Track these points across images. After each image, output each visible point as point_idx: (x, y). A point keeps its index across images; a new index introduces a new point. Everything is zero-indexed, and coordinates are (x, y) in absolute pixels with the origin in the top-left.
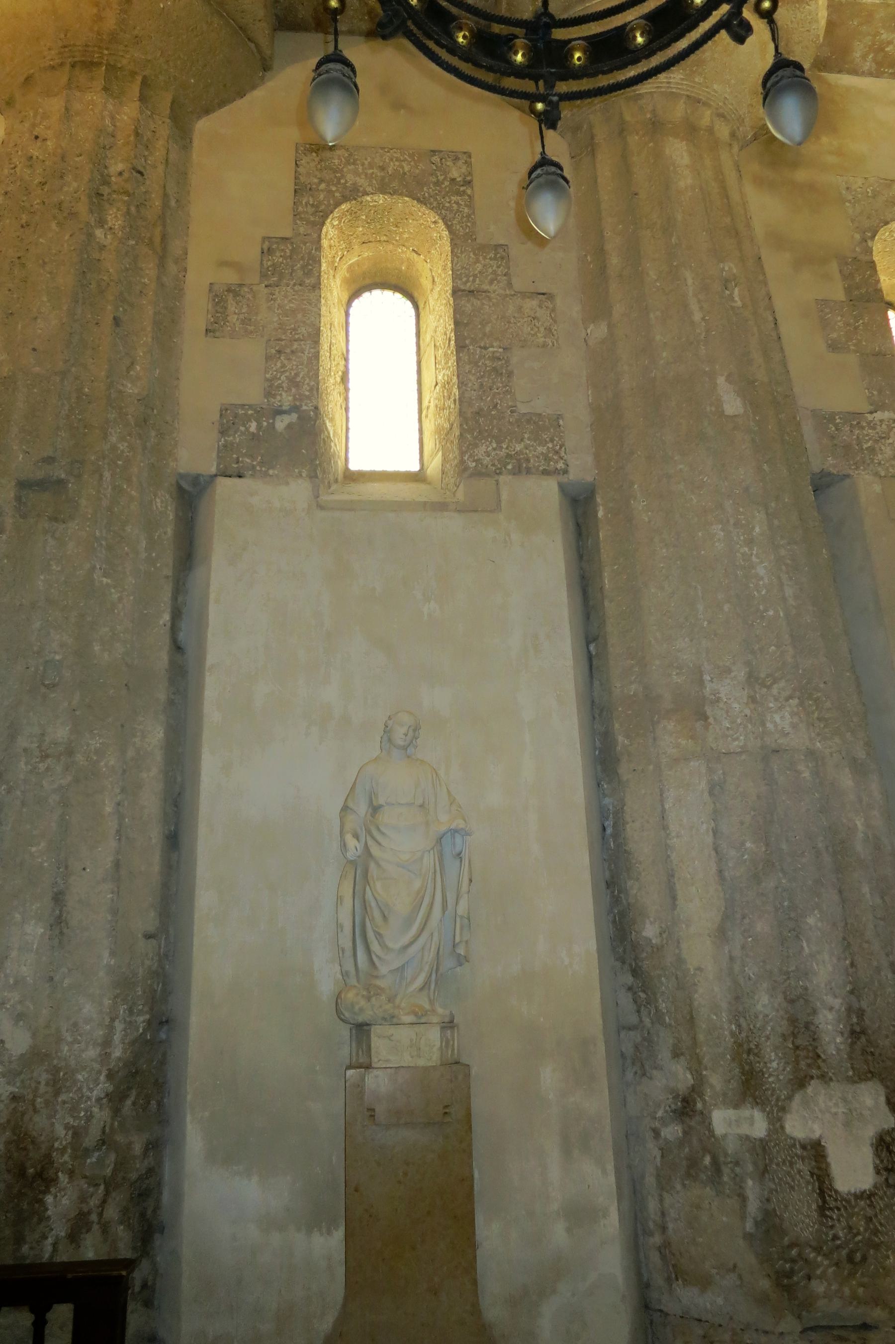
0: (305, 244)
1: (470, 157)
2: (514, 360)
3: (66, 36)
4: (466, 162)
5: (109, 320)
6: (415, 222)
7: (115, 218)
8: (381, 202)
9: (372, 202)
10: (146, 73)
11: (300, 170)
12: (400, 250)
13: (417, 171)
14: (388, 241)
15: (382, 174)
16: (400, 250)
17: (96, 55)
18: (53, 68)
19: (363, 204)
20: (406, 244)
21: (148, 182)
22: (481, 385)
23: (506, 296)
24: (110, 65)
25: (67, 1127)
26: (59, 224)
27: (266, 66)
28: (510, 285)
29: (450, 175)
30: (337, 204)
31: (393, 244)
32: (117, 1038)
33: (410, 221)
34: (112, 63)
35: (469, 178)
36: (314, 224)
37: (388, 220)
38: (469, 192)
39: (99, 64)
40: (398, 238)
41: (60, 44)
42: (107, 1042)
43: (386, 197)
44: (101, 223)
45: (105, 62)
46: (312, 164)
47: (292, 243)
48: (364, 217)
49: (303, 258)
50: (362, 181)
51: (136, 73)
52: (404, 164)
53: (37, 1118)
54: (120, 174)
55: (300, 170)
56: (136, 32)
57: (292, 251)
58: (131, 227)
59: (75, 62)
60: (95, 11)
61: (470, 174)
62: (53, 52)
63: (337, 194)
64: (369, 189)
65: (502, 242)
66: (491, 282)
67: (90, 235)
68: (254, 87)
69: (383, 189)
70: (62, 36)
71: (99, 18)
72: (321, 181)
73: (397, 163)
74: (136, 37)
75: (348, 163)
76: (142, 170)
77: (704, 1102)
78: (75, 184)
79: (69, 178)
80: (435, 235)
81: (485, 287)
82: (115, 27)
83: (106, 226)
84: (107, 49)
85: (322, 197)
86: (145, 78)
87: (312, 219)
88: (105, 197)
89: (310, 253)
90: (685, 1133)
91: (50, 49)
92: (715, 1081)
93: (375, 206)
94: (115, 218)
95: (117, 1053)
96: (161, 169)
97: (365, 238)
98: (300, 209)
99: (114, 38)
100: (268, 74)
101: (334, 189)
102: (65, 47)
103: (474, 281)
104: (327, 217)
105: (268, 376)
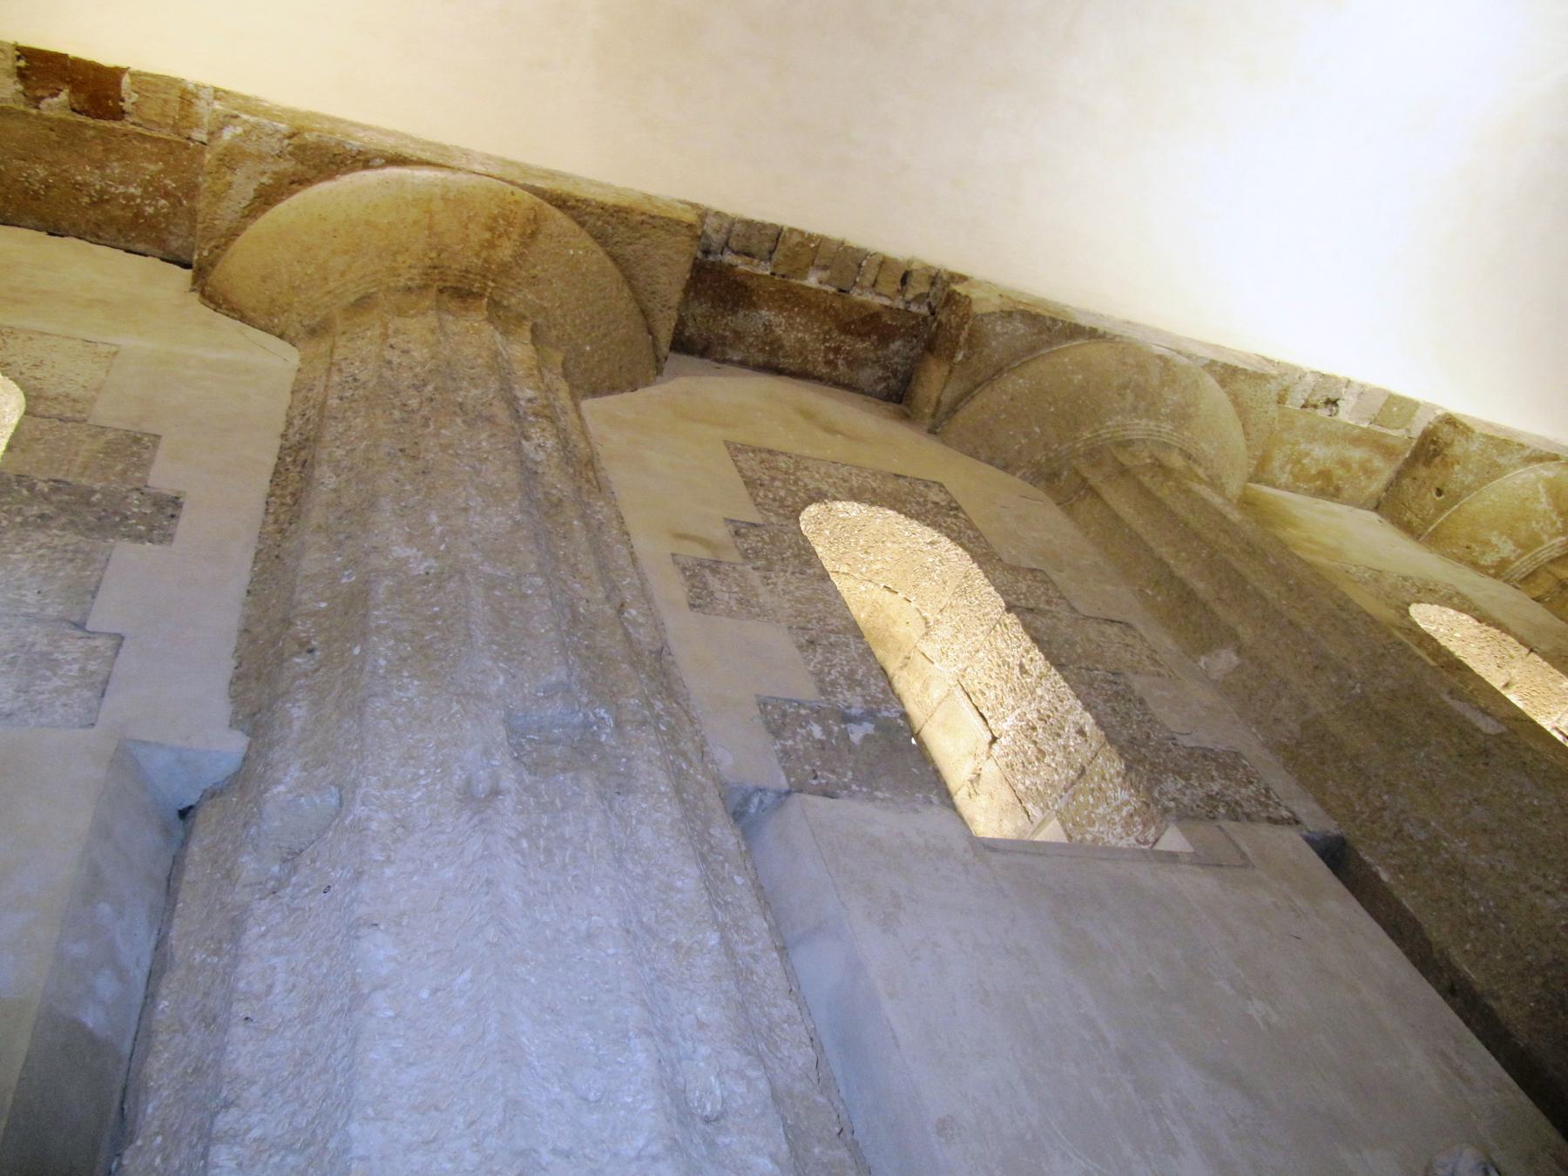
3: (439, 255)
6: (896, 546)
8: (854, 514)
9: (842, 512)
10: (539, 320)
12: (863, 589)
14: (848, 574)
16: (863, 589)
17: (477, 285)
18: (409, 289)
19: (832, 513)
20: (876, 579)
24: (494, 301)
27: (658, 367)
31: (855, 579)
33: (889, 545)
34: (497, 298)
37: (857, 543)
39: (481, 296)
40: (864, 570)
41: (428, 262)
43: (862, 508)
45: (488, 295)
48: (827, 532)
51: (524, 317)
56: (533, 272)
59: (445, 288)
60: (488, 235)
62: (414, 271)
68: (647, 385)
69: (855, 496)
70: (433, 255)
71: (491, 245)
74: (534, 277)
80: (931, 560)
82: (510, 259)
84: (493, 281)
86: (535, 325)
91: (410, 267)
93: (844, 520)
99: (505, 269)
100: (658, 378)
102: (435, 268)
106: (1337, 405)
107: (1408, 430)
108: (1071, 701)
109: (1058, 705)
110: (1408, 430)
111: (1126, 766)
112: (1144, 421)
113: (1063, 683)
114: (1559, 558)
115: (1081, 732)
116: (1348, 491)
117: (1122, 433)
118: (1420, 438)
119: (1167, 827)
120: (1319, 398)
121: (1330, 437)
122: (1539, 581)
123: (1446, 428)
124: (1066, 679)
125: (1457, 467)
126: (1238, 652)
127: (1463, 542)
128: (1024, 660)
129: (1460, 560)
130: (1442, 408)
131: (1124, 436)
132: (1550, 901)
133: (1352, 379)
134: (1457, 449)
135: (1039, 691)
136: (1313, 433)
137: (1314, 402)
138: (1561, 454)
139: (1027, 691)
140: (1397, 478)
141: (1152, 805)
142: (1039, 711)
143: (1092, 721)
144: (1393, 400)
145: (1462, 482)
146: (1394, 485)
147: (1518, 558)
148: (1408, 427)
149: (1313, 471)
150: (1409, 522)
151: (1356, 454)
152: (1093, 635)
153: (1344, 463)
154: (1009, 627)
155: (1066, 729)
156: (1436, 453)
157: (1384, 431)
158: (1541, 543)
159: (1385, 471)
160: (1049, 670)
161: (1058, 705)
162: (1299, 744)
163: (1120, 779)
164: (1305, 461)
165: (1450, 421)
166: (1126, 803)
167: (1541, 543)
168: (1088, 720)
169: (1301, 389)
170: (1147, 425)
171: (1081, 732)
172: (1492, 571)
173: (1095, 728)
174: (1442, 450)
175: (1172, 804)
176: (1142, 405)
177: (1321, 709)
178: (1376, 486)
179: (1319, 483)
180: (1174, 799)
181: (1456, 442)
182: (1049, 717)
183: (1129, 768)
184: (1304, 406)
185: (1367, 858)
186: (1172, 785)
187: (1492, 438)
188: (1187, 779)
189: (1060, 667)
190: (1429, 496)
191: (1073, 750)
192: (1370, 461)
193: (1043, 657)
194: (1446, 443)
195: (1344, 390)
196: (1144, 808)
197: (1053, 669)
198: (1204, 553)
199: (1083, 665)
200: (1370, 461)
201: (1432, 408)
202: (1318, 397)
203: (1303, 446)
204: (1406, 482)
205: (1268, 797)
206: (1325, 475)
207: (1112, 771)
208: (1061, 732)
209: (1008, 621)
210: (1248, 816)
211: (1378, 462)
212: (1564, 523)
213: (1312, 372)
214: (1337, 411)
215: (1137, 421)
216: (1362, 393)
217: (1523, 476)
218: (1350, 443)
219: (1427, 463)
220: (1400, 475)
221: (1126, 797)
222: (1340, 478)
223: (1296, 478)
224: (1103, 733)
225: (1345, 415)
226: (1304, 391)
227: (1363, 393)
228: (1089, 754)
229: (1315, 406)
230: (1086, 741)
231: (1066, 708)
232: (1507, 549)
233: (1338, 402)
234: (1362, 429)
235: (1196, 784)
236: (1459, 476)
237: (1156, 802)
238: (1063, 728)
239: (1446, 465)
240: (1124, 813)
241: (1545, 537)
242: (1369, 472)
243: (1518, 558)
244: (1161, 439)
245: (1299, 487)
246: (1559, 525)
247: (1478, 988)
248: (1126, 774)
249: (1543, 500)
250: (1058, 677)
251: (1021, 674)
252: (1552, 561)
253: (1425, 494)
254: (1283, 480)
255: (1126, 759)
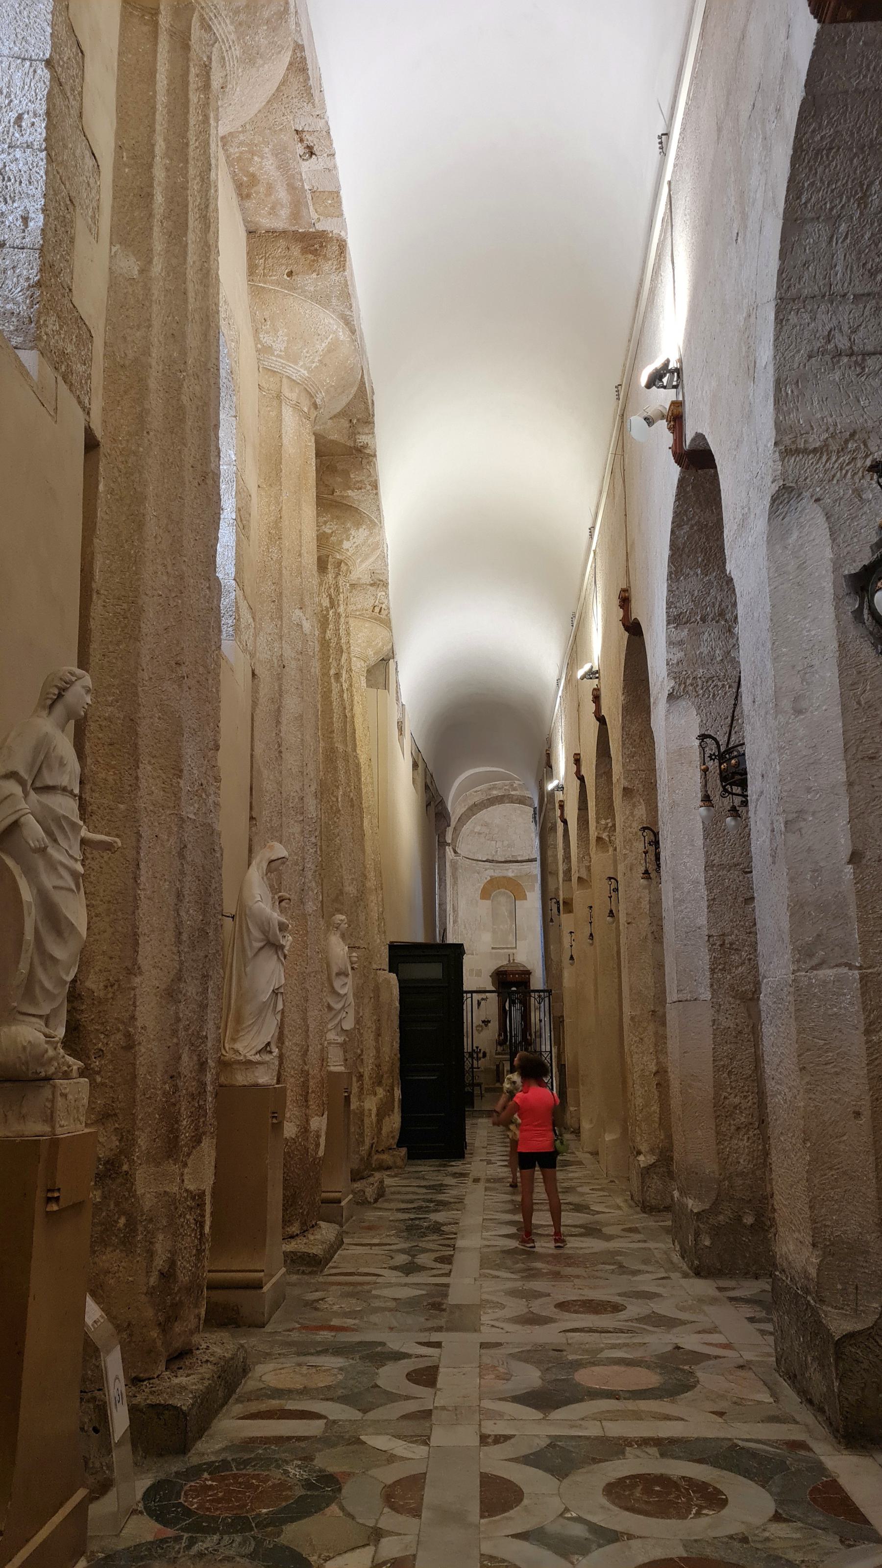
77: (132, 1162)
90: (104, 1197)
92: (143, 1141)
106: (311, 156)
107: (319, 219)
108: (38, 190)
109: (25, 182)
110: (319, 219)
111: (39, 281)
112: (231, 28)
113: (42, 173)
114: (294, 380)
115: (25, 220)
116: (250, 204)
117: (212, 15)
118: (318, 232)
119: (32, 348)
120: (310, 139)
121: (283, 166)
122: (272, 379)
123: (335, 247)
124: (46, 173)
125: (314, 275)
126: (142, 271)
127: (267, 314)
128: (26, 116)
129: (253, 321)
130: (347, 234)
131: (211, 19)
132: (165, 578)
133: (336, 156)
134: (326, 267)
135: (18, 153)
136: (280, 152)
137: (305, 138)
138: (357, 332)
139: (8, 141)
140: (281, 233)
141: (33, 325)
142: (5, 166)
143: (41, 224)
144: (335, 195)
145: (305, 285)
146: (275, 234)
147: (278, 356)
148: (322, 218)
149: (251, 170)
150: (257, 266)
151: (282, 194)
152: (78, 152)
153: (270, 188)
154: (37, 77)
155: (16, 205)
156: (315, 252)
157: (310, 203)
158: (296, 363)
159: (280, 223)
160: (41, 151)
161: (25, 182)
162: (123, 366)
163: (26, 284)
164: (256, 158)
165: (342, 247)
166: (18, 304)
167: (296, 363)
168: (37, 221)
169: (309, 121)
170: (230, 33)
171: (25, 220)
172: (259, 346)
173: (39, 232)
174: (319, 255)
175: (45, 337)
176: (242, 17)
177: (154, 364)
178: (266, 222)
179: (245, 179)
180: (47, 334)
181: (330, 262)
182: (9, 180)
183: (39, 284)
184: (297, 131)
185: (101, 469)
186: (52, 324)
187: (346, 285)
188: (61, 327)
189: (50, 159)
190: (284, 267)
191: (7, 223)
192: (282, 206)
193: (44, 135)
194: (325, 255)
195: (325, 155)
196: (27, 321)
197: (44, 153)
198: (180, 180)
199: (60, 171)
200: (282, 206)
201: (344, 227)
202: (310, 139)
203: (267, 150)
204: (282, 243)
205: (86, 383)
206: (254, 180)
207: (25, 272)
208: (9, 201)
209: (39, 71)
210: (72, 384)
211: (284, 213)
212: (316, 367)
213: (327, 122)
214: (307, 160)
215: (228, 21)
216: (330, 171)
217: (332, 321)
218: (287, 185)
219: (305, 251)
220: (284, 233)
221: (20, 299)
222: (258, 193)
223: (239, 159)
224: (41, 242)
225: (307, 167)
226: (310, 125)
227: (331, 171)
228: (18, 242)
229: (301, 141)
230: (24, 231)
231: (29, 192)
232: (279, 346)
233: (314, 156)
234: (303, 186)
235: (62, 336)
236: (309, 281)
237: (38, 328)
238: (14, 202)
239: (312, 267)
240: (8, 307)
241: (301, 363)
242: (273, 211)
243: (278, 356)
244: (225, 54)
245: (233, 166)
246: (314, 365)
247: (94, 586)
248: (33, 286)
249: (324, 345)
250: (43, 164)
251: (14, 123)
252: (288, 377)
253: (282, 264)
254: (231, 150)
255: (42, 276)
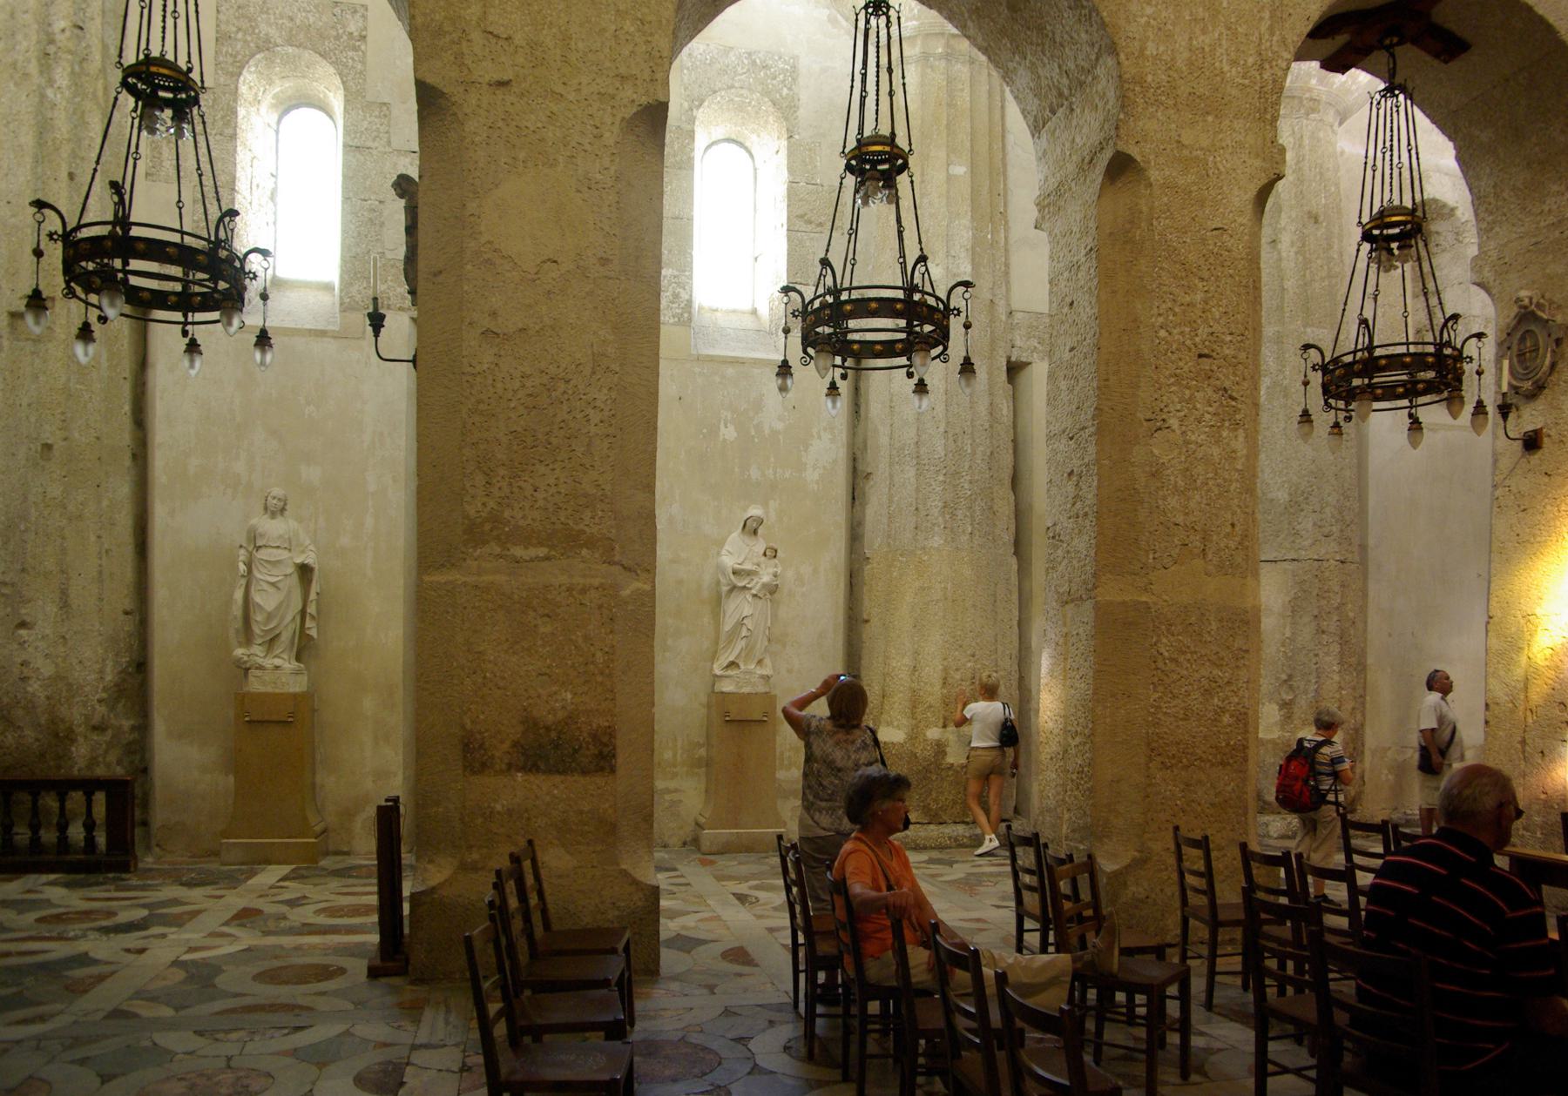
0: (224, 94)
1: (367, 10)
2: (386, 213)
4: (363, 16)
5: (64, 175)
7: (62, 77)
11: (222, 17)
13: (321, 24)
15: (290, 25)
21: (88, 36)
22: (359, 233)
23: (385, 153)
25: (81, 715)
26: (16, 84)
28: (389, 143)
29: (348, 30)
30: (252, 56)
32: (108, 670)
35: (364, 33)
36: (232, 74)
38: (363, 47)
42: (101, 671)
44: (51, 82)
46: (231, 11)
47: (214, 93)
49: (222, 109)
50: (273, 32)
52: (309, 15)
53: (62, 709)
54: (63, 31)
55: (222, 17)
57: (214, 100)
58: (76, 84)
61: (365, 28)
63: (252, 45)
64: (279, 41)
65: (386, 101)
66: (374, 140)
67: (43, 96)
72: (239, 29)
73: (304, 14)
75: (262, 12)
76: (81, 24)
78: (25, 44)
79: (19, 37)
81: (369, 144)
83: (56, 86)
85: (239, 47)
87: (231, 70)
88: (52, 57)
89: (228, 104)
94: (62, 77)
95: (109, 678)
96: (98, 21)
97: (283, 75)
98: (221, 59)
101: (249, 39)
103: (361, 137)
104: (244, 67)
105: (195, 218)
